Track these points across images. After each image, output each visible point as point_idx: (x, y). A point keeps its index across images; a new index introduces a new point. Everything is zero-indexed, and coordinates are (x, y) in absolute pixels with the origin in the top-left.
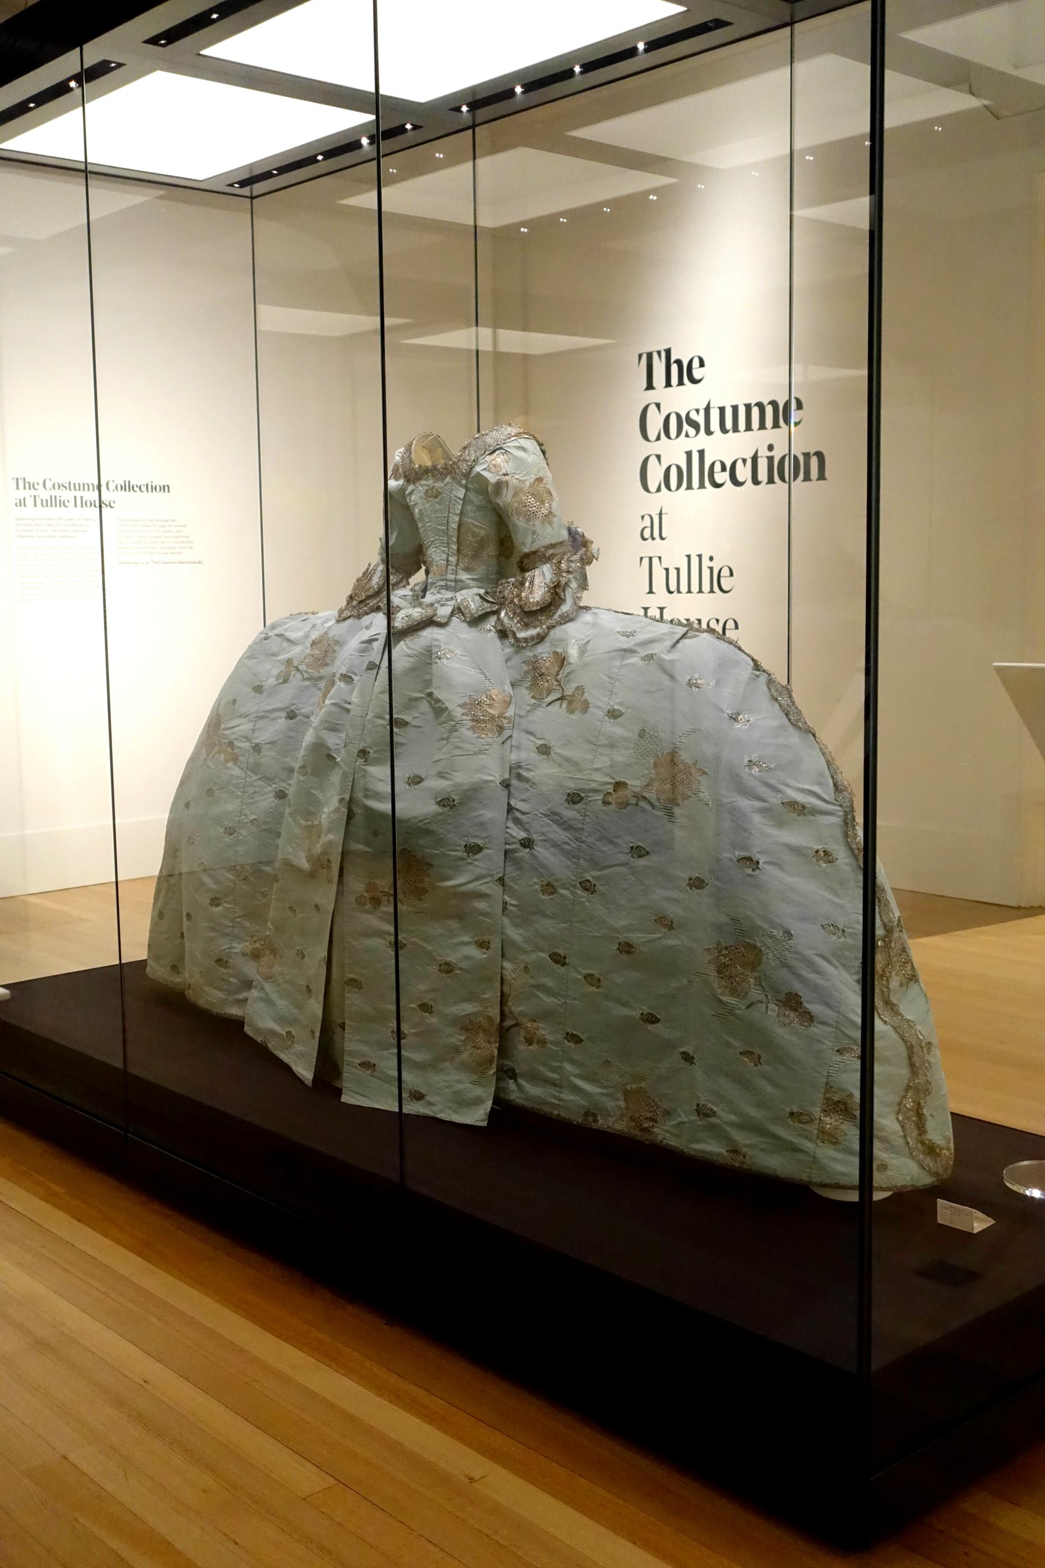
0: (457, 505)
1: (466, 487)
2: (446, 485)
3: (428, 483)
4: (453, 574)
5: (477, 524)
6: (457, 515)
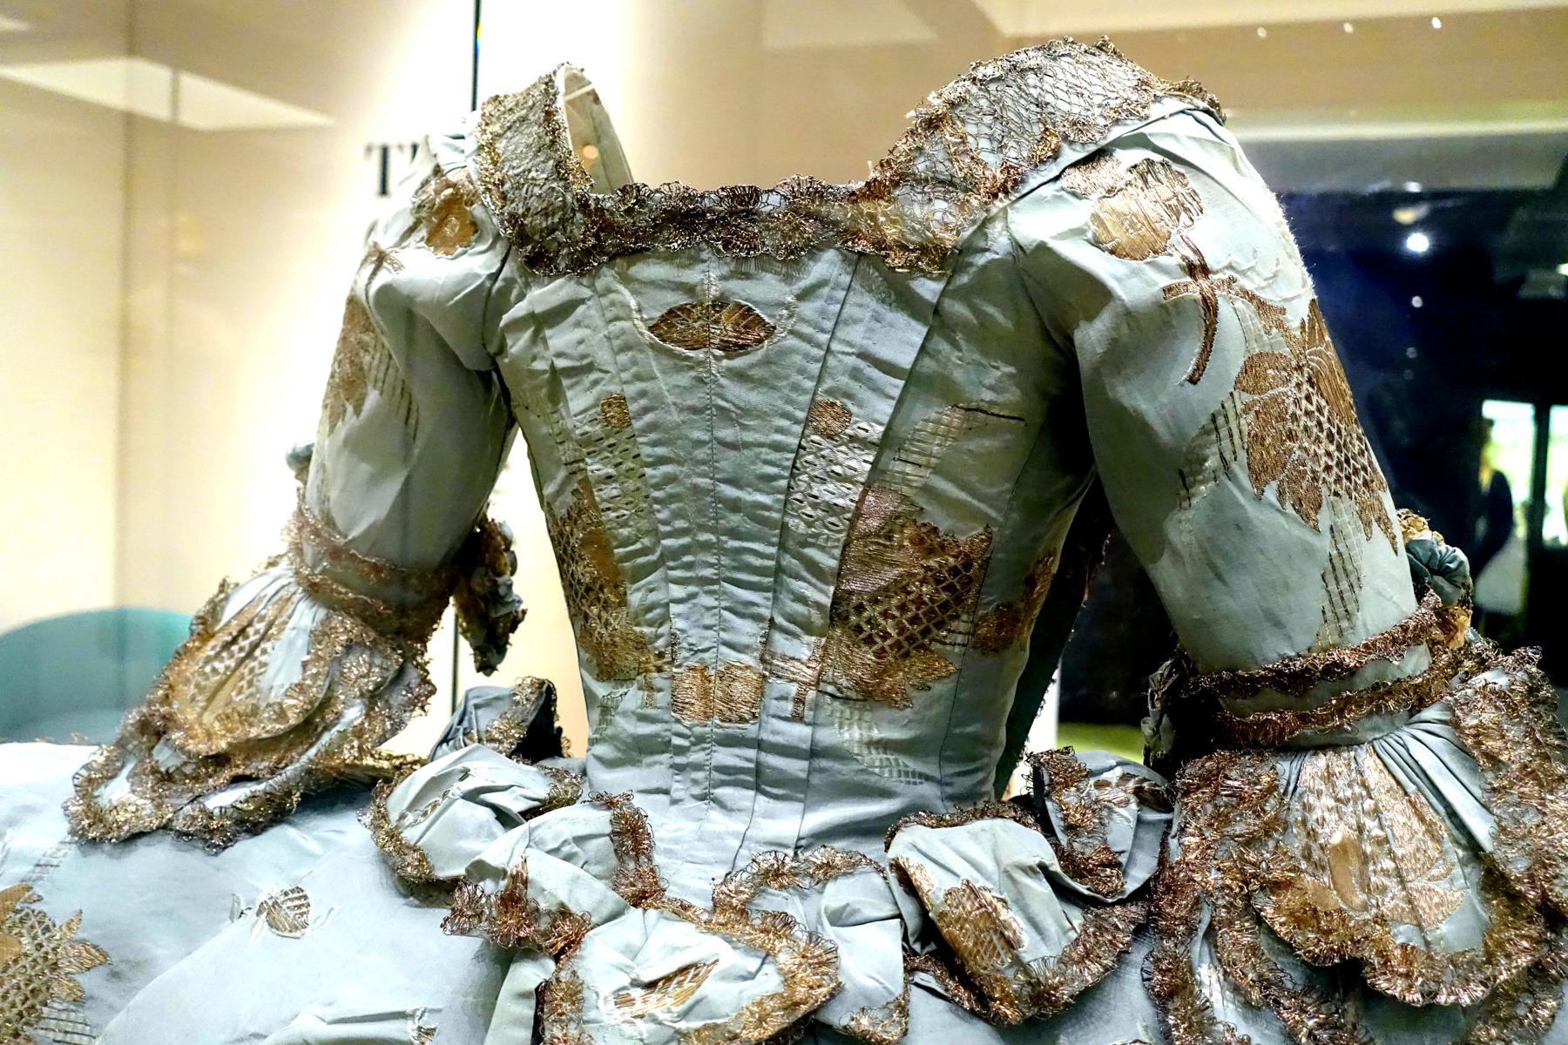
0: (864, 393)
1: (935, 318)
2: (803, 296)
3: (692, 276)
4: (797, 718)
5: (963, 496)
6: (865, 444)
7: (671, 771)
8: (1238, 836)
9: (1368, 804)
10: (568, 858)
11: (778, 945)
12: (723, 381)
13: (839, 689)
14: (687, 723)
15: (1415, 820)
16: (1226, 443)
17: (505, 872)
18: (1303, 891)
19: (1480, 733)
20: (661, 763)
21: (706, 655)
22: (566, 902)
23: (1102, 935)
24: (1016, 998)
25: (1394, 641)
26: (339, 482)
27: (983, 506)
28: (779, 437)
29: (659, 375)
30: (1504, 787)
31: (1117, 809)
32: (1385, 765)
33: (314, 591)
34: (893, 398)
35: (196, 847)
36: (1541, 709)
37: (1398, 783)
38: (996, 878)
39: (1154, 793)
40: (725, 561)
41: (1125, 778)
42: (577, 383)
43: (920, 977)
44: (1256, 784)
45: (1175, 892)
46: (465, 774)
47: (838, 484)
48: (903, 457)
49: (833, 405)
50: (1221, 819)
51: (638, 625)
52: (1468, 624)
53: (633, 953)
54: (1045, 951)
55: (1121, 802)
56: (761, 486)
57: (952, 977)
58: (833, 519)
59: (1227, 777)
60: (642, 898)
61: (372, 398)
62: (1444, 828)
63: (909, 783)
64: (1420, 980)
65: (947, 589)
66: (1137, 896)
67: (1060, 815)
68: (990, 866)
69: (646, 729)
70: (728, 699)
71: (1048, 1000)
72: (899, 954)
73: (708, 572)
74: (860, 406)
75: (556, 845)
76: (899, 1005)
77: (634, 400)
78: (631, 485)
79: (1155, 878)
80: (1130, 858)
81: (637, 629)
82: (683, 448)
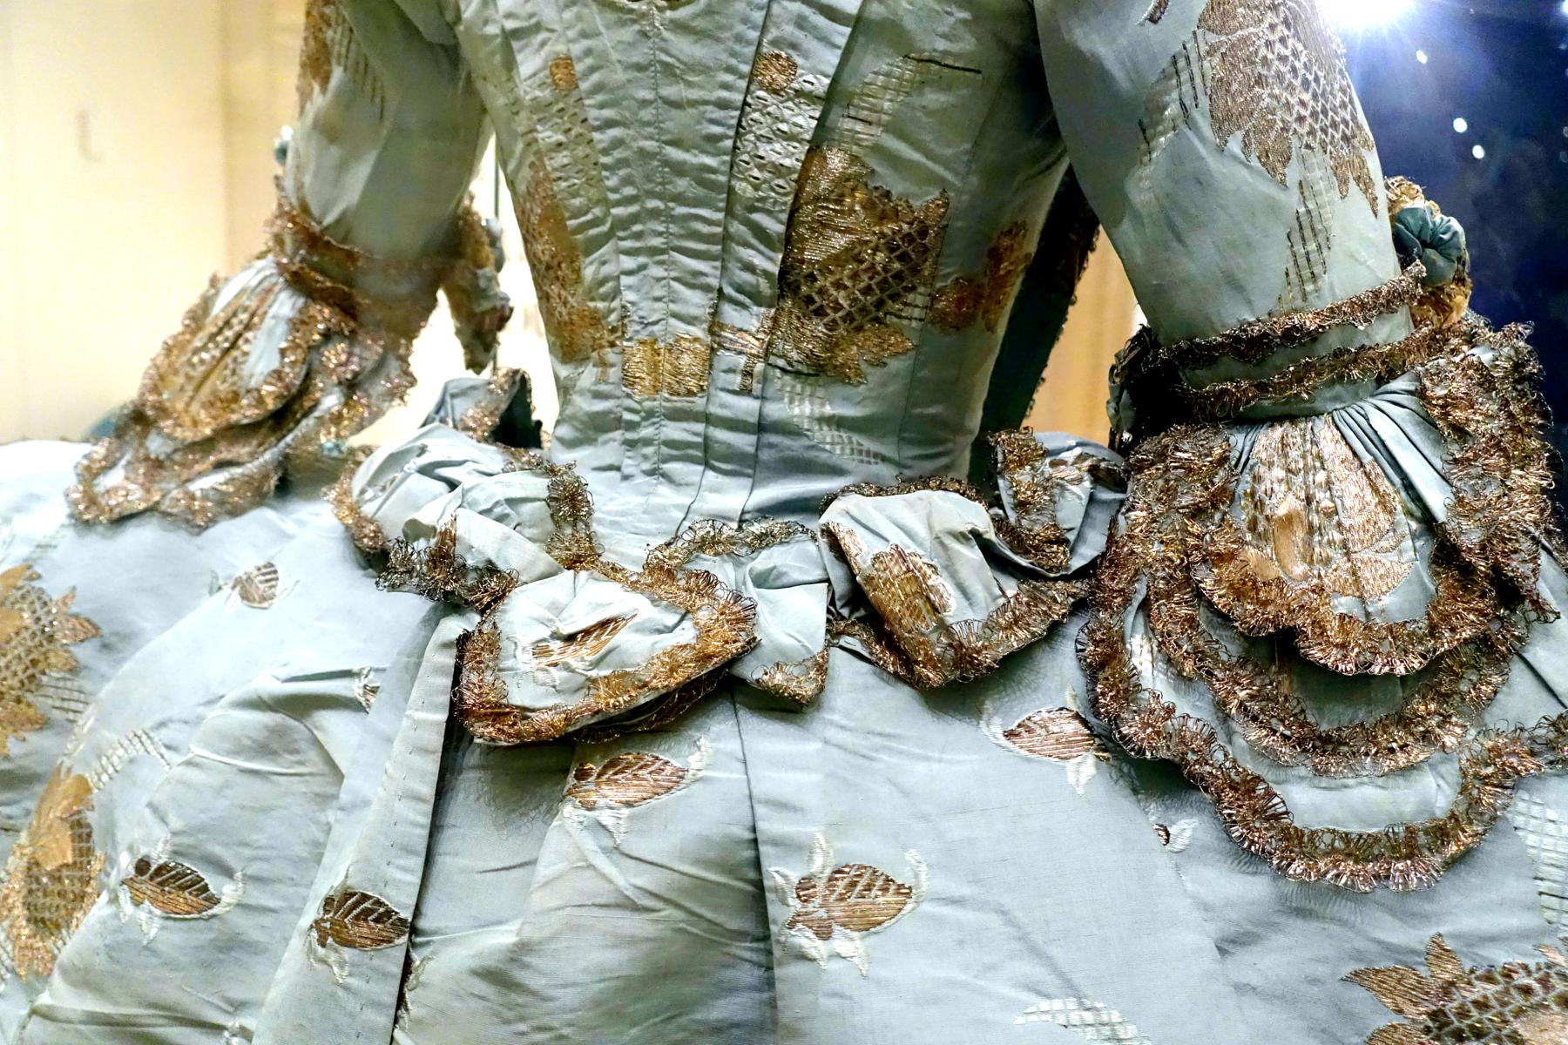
0: (810, 43)
4: (745, 391)
5: (917, 156)
6: (811, 98)
7: (624, 447)
8: (1183, 508)
9: (1321, 477)
10: (501, 519)
11: (698, 603)
12: (666, 34)
13: (790, 364)
14: (637, 398)
15: (1368, 491)
16: (1186, 88)
17: (434, 529)
18: (1245, 563)
19: (1449, 403)
20: (614, 440)
21: (656, 328)
22: (494, 560)
23: (1036, 606)
24: (940, 661)
25: (1363, 306)
26: (311, 167)
27: (939, 169)
28: (724, 94)
29: (602, 30)
30: (1468, 459)
31: (1070, 487)
32: (1343, 436)
33: (297, 281)
34: (839, 48)
35: (179, 528)
36: (1526, 386)
37: (1355, 454)
38: (928, 544)
39: (1108, 471)
40: (673, 228)
41: (1081, 458)
42: (526, 46)
43: (846, 641)
44: (1207, 456)
45: (1117, 566)
46: (423, 450)
47: (785, 143)
48: (853, 113)
49: (778, 57)
50: (1169, 493)
51: (592, 299)
52: (1466, 304)
53: (557, 609)
54: (970, 615)
55: (1072, 480)
56: (708, 147)
57: (879, 642)
58: (781, 182)
59: (1177, 449)
60: (575, 562)
61: (337, 74)
62: (1399, 500)
63: (862, 461)
64: (1356, 650)
65: (901, 258)
66: (1081, 574)
67: (1011, 492)
68: (922, 532)
69: (600, 406)
70: (677, 372)
71: (971, 663)
72: (823, 616)
73: (657, 242)
74: (806, 57)
75: (488, 506)
76: (817, 663)
77: (580, 59)
78: (581, 151)
79: (1103, 555)
80: (1079, 537)
81: (592, 304)
82: (628, 108)
